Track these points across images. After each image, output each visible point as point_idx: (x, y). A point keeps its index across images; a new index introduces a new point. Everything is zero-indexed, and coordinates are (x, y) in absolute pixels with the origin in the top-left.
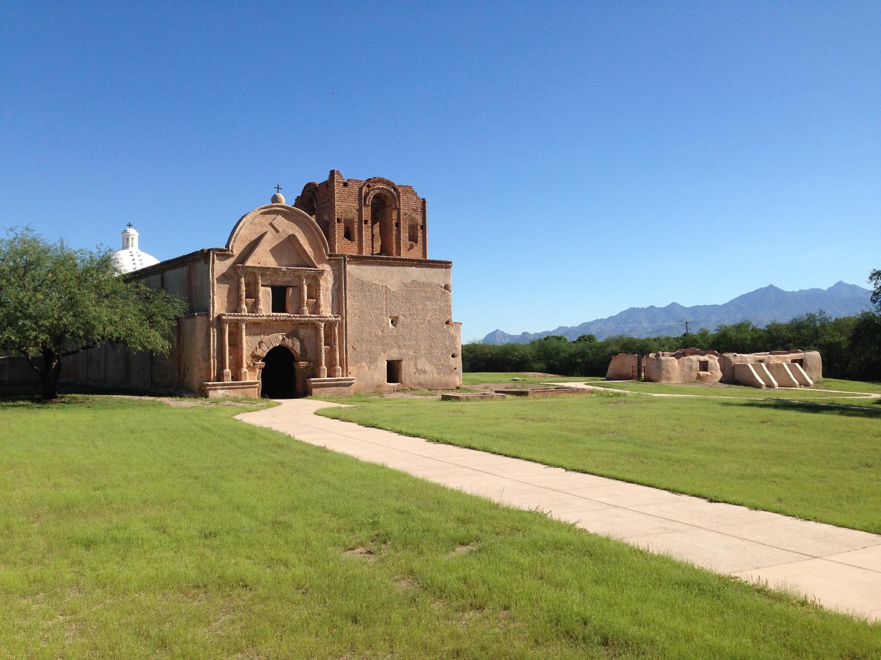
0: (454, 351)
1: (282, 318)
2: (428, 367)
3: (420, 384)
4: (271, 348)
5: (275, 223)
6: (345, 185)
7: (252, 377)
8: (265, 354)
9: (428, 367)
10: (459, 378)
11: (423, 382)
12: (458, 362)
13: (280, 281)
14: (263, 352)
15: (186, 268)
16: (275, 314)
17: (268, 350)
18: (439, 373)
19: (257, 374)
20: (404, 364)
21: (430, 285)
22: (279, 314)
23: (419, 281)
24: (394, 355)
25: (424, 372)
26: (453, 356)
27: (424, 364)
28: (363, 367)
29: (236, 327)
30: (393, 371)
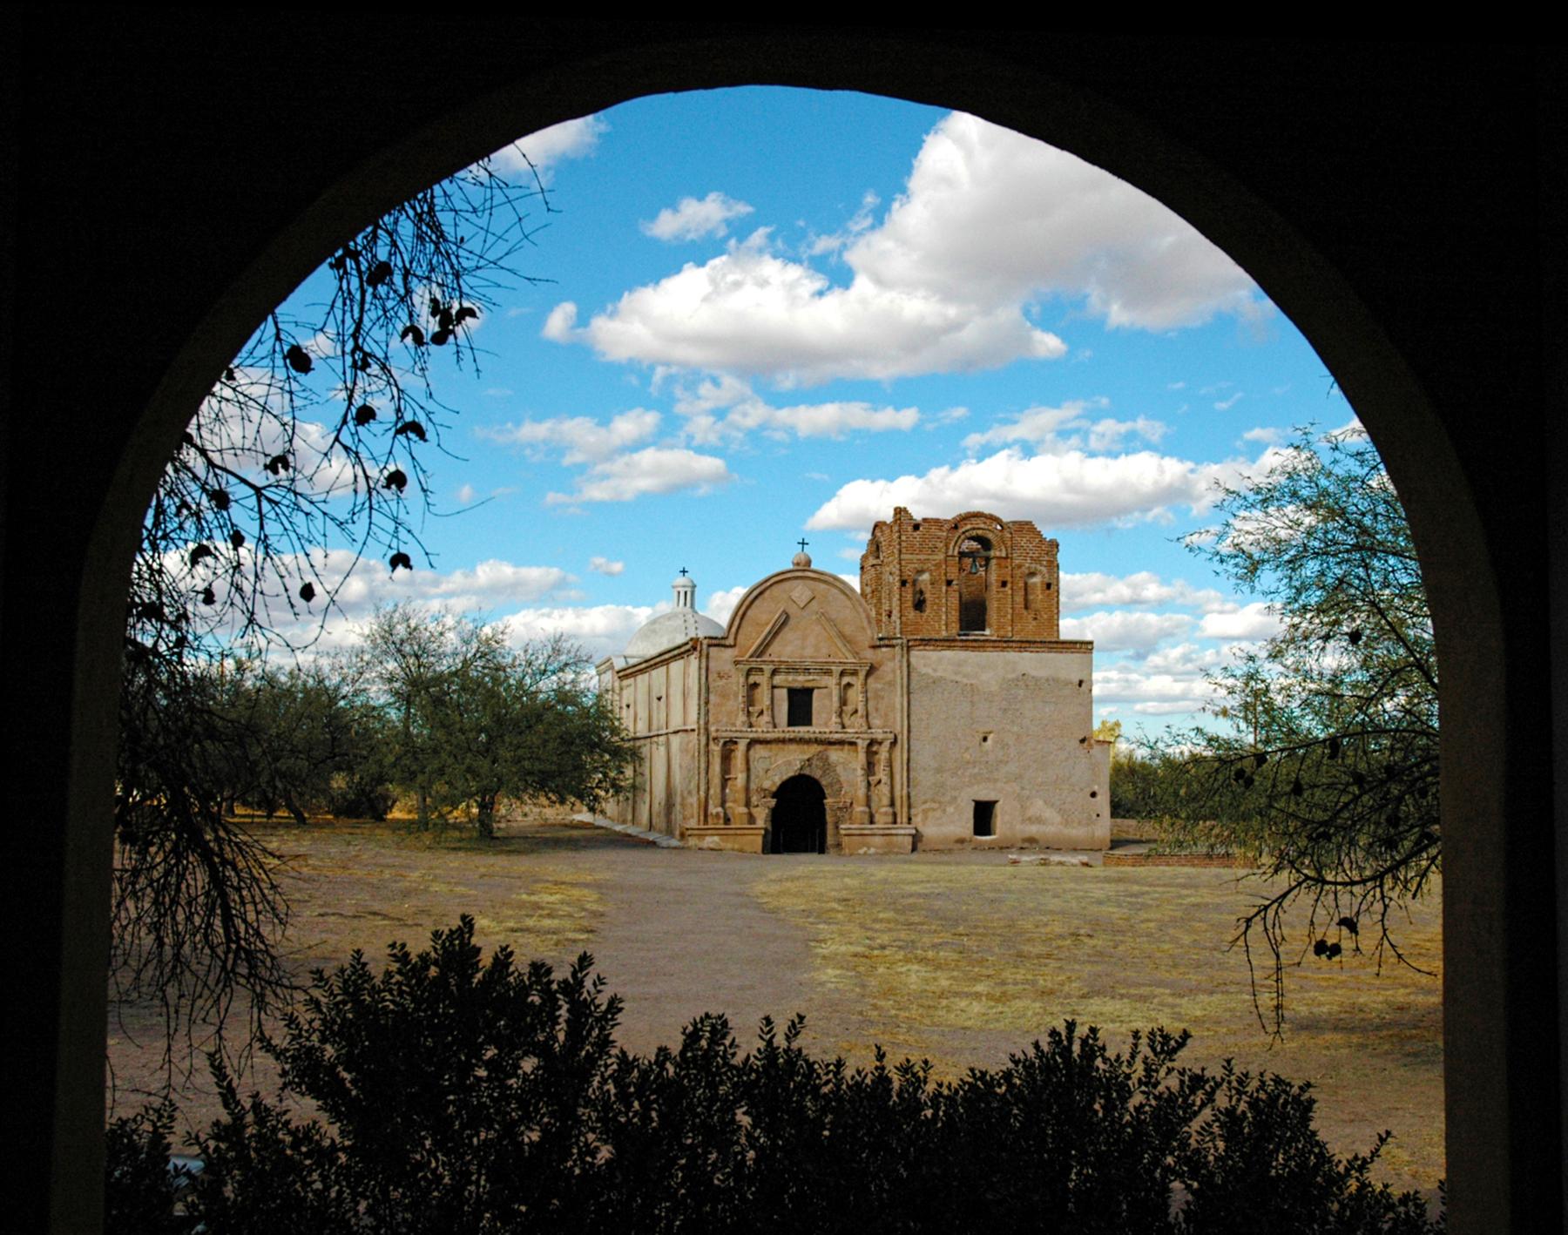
0: (1096, 788)
1: (801, 735)
2: (1049, 814)
3: (1032, 840)
4: (785, 777)
5: (795, 595)
6: (916, 527)
7: (762, 816)
8: (774, 789)
9: (1049, 814)
10: (1104, 827)
11: (1037, 837)
12: (1103, 803)
13: (800, 681)
14: (774, 781)
15: (681, 662)
16: (791, 729)
17: (779, 783)
18: (1067, 823)
19: (764, 816)
20: (998, 808)
21: (1054, 681)
22: (797, 729)
23: (1034, 673)
24: (985, 796)
25: (1039, 820)
26: (1093, 795)
27: (1038, 807)
28: (934, 810)
29: (729, 745)
30: (983, 815)
